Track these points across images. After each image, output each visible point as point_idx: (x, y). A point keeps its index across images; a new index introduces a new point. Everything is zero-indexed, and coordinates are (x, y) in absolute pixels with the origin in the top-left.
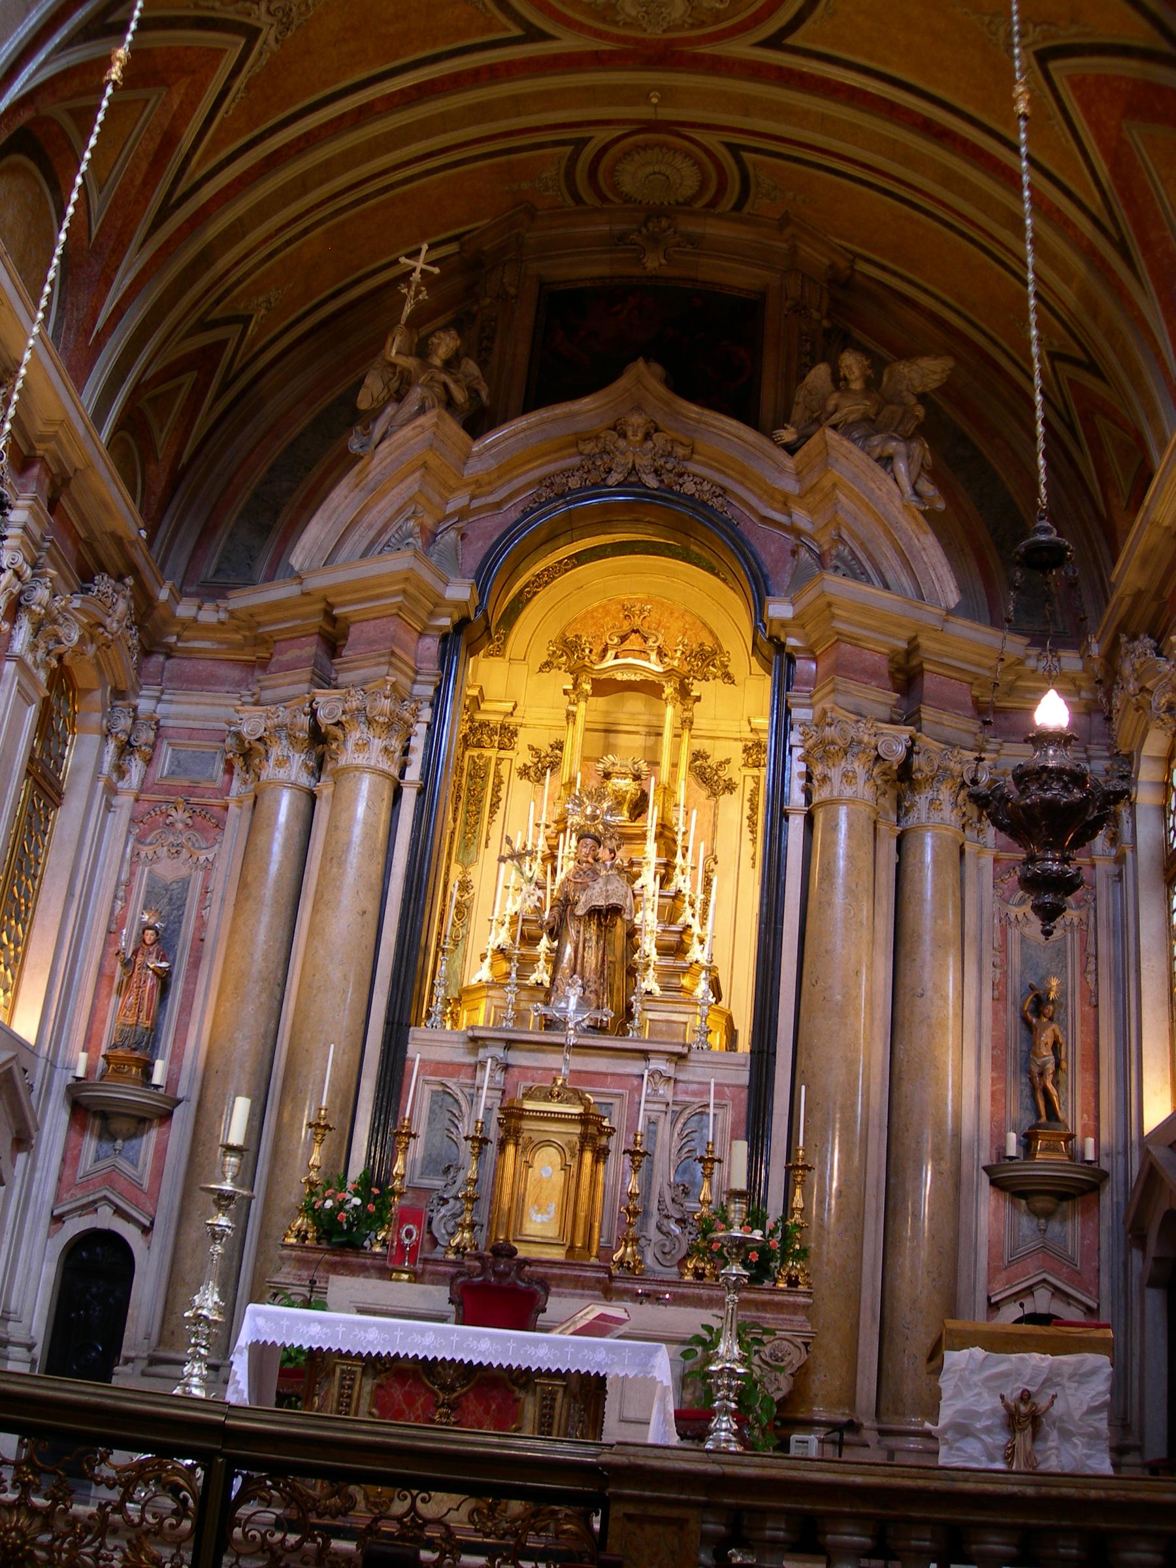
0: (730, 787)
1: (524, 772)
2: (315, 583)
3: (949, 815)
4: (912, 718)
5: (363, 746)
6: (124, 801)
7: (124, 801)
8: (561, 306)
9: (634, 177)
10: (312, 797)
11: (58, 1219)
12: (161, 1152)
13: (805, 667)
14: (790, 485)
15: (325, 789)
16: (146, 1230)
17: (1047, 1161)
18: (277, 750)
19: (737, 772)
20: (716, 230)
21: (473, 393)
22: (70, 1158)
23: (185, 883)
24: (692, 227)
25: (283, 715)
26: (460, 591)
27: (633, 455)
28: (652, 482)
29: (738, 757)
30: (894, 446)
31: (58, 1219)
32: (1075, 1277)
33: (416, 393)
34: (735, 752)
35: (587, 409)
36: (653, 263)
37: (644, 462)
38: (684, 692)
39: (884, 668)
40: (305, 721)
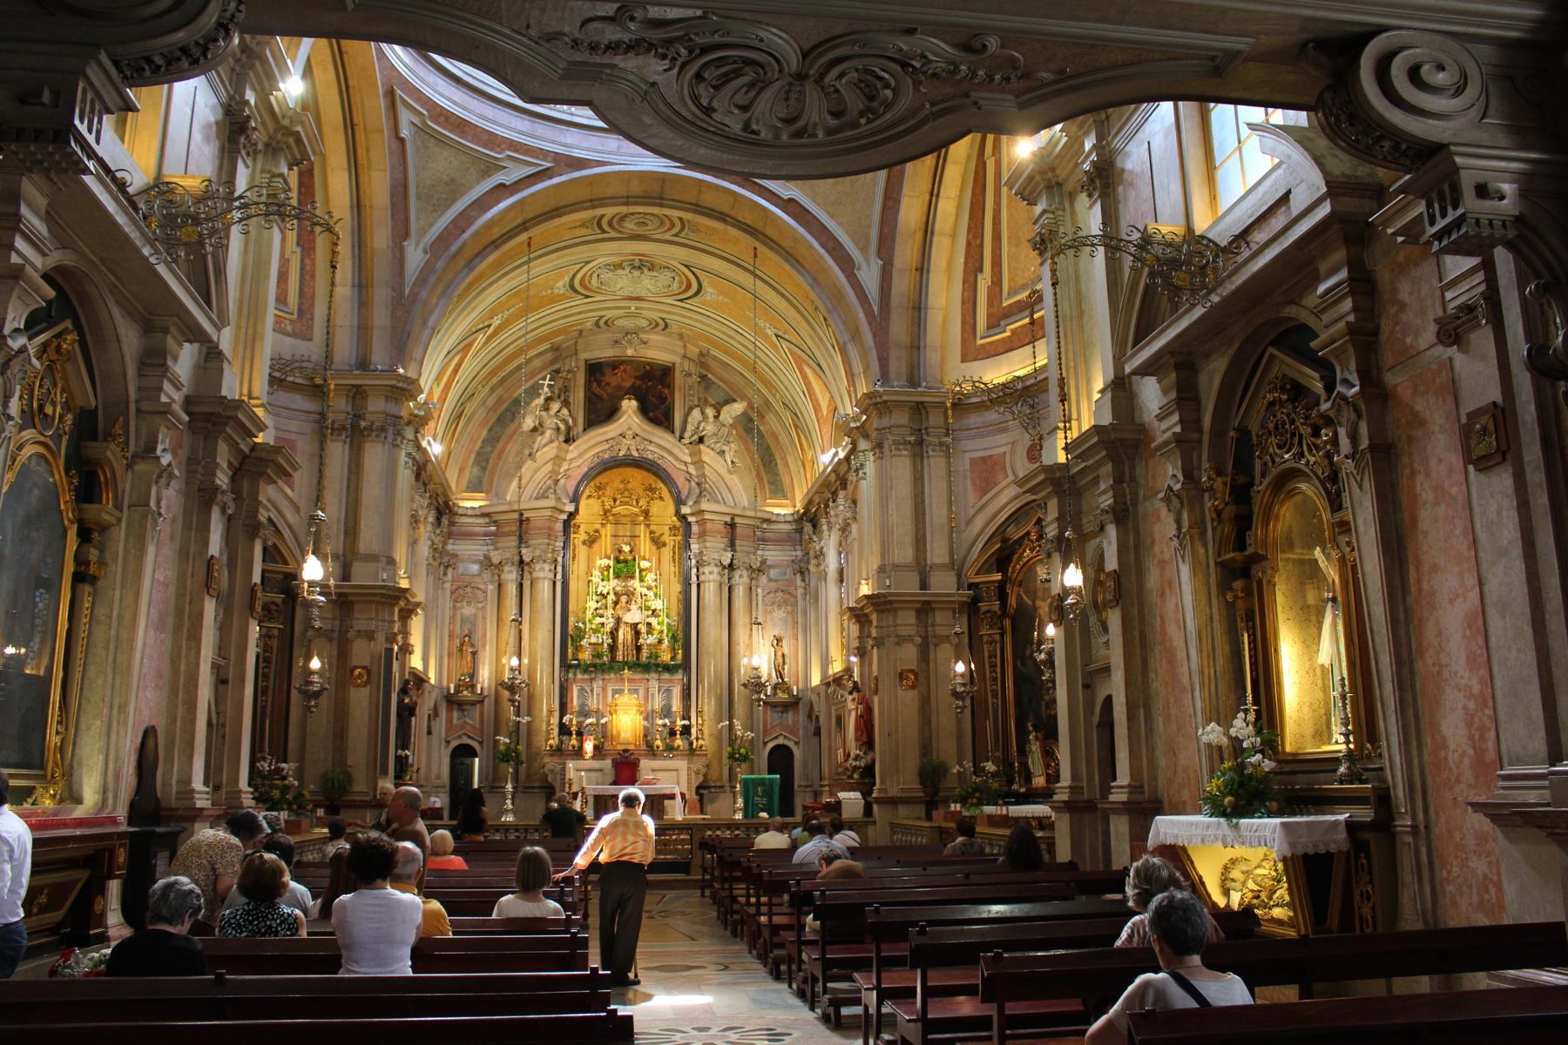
0: (664, 544)
1: (584, 543)
2: (516, 507)
3: (746, 579)
4: (732, 545)
5: (542, 569)
6: (448, 585)
7: (448, 585)
8: (594, 370)
9: (619, 323)
10: (521, 586)
11: (448, 742)
12: (482, 714)
13: (695, 528)
14: (688, 459)
15: (527, 584)
16: (481, 743)
17: (782, 696)
18: (507, 568)
19: (667, 538)
20: (655, 337)
21: (564, 421)
22: (450, 720)
23: (475, 616)
24: (643, 336)
25: (508, 555)
26: (570, 508)
27: (628, 447)
28: (635, 454)
29: (667, 532)
30: (726, 448)
31: (448, 742)
32: (793, 732)
33: (548, 433)
34: (666, 530)
35: (610, 430)
36: (630, 352)
37: (633, 448)
38: (646, 513)
39: (722, 527)
40: (517, 558)
